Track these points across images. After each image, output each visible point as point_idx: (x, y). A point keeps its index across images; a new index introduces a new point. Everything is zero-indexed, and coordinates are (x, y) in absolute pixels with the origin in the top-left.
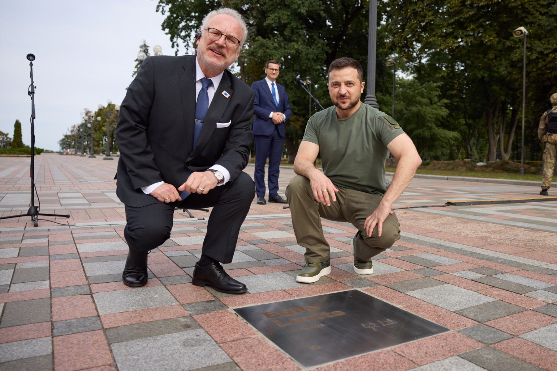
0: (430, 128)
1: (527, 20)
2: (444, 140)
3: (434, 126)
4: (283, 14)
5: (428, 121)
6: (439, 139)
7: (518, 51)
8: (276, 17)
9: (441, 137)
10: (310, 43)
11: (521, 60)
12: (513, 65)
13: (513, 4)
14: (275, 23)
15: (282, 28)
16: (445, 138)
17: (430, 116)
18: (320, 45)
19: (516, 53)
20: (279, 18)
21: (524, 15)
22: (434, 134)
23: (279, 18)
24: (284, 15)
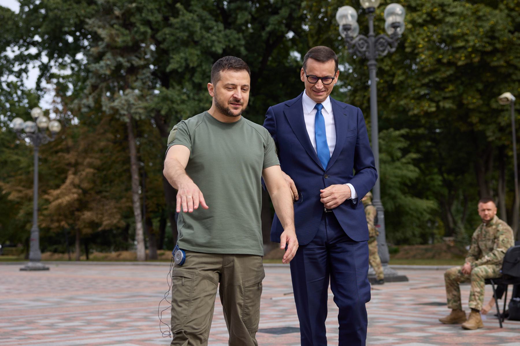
1: (514, 77)
2: (415, 214)
3: (399, 194)
4: (191, 54)
5: (390, 187)
6: (407, 213)
7: (506, 114)
8: (182, 58)
9: (410, 209)
11: (509, 125)
12: (502, 129)
13: (495, 64)
14: (180, 67)
16: (417, 210)
17: (393, 179)
19: (504, 117)
20: (186, 60)
21: (511, 71)
22: (400, 206)
23: (186, 60)
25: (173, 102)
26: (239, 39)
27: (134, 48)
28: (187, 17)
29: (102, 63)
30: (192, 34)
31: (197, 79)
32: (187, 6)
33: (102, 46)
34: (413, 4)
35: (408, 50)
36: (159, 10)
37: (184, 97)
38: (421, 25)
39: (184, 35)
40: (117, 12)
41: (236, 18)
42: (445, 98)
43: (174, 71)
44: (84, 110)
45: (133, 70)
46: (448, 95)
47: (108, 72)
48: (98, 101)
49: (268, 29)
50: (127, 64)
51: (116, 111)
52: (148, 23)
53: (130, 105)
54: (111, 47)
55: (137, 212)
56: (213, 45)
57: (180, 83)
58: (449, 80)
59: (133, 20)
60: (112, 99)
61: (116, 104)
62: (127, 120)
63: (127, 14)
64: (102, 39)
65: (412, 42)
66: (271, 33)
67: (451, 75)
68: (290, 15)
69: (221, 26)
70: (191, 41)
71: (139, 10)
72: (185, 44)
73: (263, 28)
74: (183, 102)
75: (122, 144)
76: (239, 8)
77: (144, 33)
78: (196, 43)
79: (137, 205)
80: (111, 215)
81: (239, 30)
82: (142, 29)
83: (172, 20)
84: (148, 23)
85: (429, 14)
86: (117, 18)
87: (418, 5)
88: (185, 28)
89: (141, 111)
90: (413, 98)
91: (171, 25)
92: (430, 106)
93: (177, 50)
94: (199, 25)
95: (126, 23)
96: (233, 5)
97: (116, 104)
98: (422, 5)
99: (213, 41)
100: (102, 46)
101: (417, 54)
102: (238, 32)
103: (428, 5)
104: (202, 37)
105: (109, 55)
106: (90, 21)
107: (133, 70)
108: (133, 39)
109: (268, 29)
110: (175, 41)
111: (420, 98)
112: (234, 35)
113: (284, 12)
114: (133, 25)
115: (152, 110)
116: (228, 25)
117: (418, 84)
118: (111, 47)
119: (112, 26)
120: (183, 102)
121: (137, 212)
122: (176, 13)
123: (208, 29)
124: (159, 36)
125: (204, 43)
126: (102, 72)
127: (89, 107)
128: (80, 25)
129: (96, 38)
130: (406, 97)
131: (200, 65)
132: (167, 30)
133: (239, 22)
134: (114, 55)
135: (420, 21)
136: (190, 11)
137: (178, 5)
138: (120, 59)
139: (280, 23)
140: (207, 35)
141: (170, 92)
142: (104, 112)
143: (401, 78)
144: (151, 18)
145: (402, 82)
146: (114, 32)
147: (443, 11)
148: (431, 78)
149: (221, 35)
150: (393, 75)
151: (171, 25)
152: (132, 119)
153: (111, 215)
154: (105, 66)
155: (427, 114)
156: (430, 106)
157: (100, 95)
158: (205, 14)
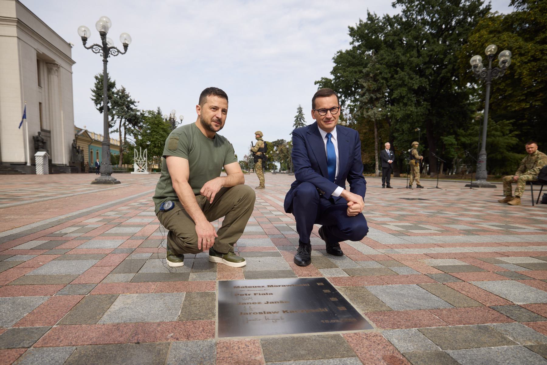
0: (502, 153)
4: (403, 90)
10: (418, 104)
15: (402, 97)
18: (425, 106)
23: (400, 93)
24: (403, 91)
25: (393, 111)
26: (426, 82)
27: (379, 90)
28: (402, 74)
29: (364, 97)
30: (404, 81)
31: (405, 101)
32: (402, 69)
33: (365, 90)
34: (523, 52)
35: (516, 77)
36: (390, 73)
37: (399, 109)
38: (526, 63)
39: (400, 82)
40: (371, 75)
41: (425, 72)
42: (536, 101)
43: (395, 98)
44: (357, 117)
45: (377, 99)
46: (538, 99)
47: (366, 101)
48: (362, 114)
49: (441, 76)
50: (374, 97)
51: (369, 116)
52: (383, 78)
53: (375, 114)
54: (368, 90)
55: (377, 157)
56: (413, 85)
57: (398, 103)
58: (541, 90)
59: (378, 78)
60: (367, 112)
61: (369, 113)
62: (373, 120)
63: (375, 75)
64: (364, 87)
65: (519, 73)
66: (443, 78)
67: (542, 88)
68: (453, 68)
69: (418, 77)
70: (403, 85)
71: (381, 73)
72: (400, 86)
73: (439, 76)
74: (398, 111)
75: (372, 131)
76: (427, 68)
77: (383, 83)
78: (406, 85)
79: (377, 154)
80: (366, 159)
81: (427, 77)
82: (382, 81)
83: (395, 76)
84: (383, 78)
85: (532, 56)
86: (371, 77)
87: (526, 52)
88: (401, 79)
89: (379, 116)
90: (516, 102)
91: (395, 79)
92: (526, 105)
93: (397, 89)
94: (407, 77)
95: (375, 79)
96: (424, 67)
97: (369, 113)
98: (529, 52)
99: (413, 84)
100: (365, 90)
101: (522, 79)
102: (426, 78)
103: (533, 51)
104: (409, 82)
105: (367, 94)
106: (360, 80)
107: (377, 99)
108: (378, 86)
109: (441, 76)
110: (396, 85)
111: (521, 101)
112: (424, 79)
113: (450, 67)
114: (378, 80)
115: (384, 116)
116: (421, 76)
117: (520, 94)
118: (368, 90)
119: (369, 81)
120: (398, 111)
121: (377, 157)
122: (397, 72)
123: (412, 79)
124: (389, 84)
125: (409, 85)
126: (364, 101)
127: (358, 115)
128: (356, 83)
129: (362, 87)
130: (511, 102)
131: (407, 95)
132: (393, 81)
133: (427, 74)
134: (369, 93)
135: (526, 60)
136: (403, 71)
137: (398, 69)
138: (372, 95)
139: (447, 72)
140: (410, 81)
141: (393, 108)
142: (364, 117)
143: (510, 92)
144: (386, 76)
145: (510, 94)
146: (370, 84)
147: (542, 53)
148: (529, 90)
149: (417, 81)
150: (506, 91)
151: (395, 79)
152: (376, 120)
153: (366, 159)
154: (366, 98)
155: (524, 109)
156: (526, 105)
157: (363, 111)
158: (411, 72)
